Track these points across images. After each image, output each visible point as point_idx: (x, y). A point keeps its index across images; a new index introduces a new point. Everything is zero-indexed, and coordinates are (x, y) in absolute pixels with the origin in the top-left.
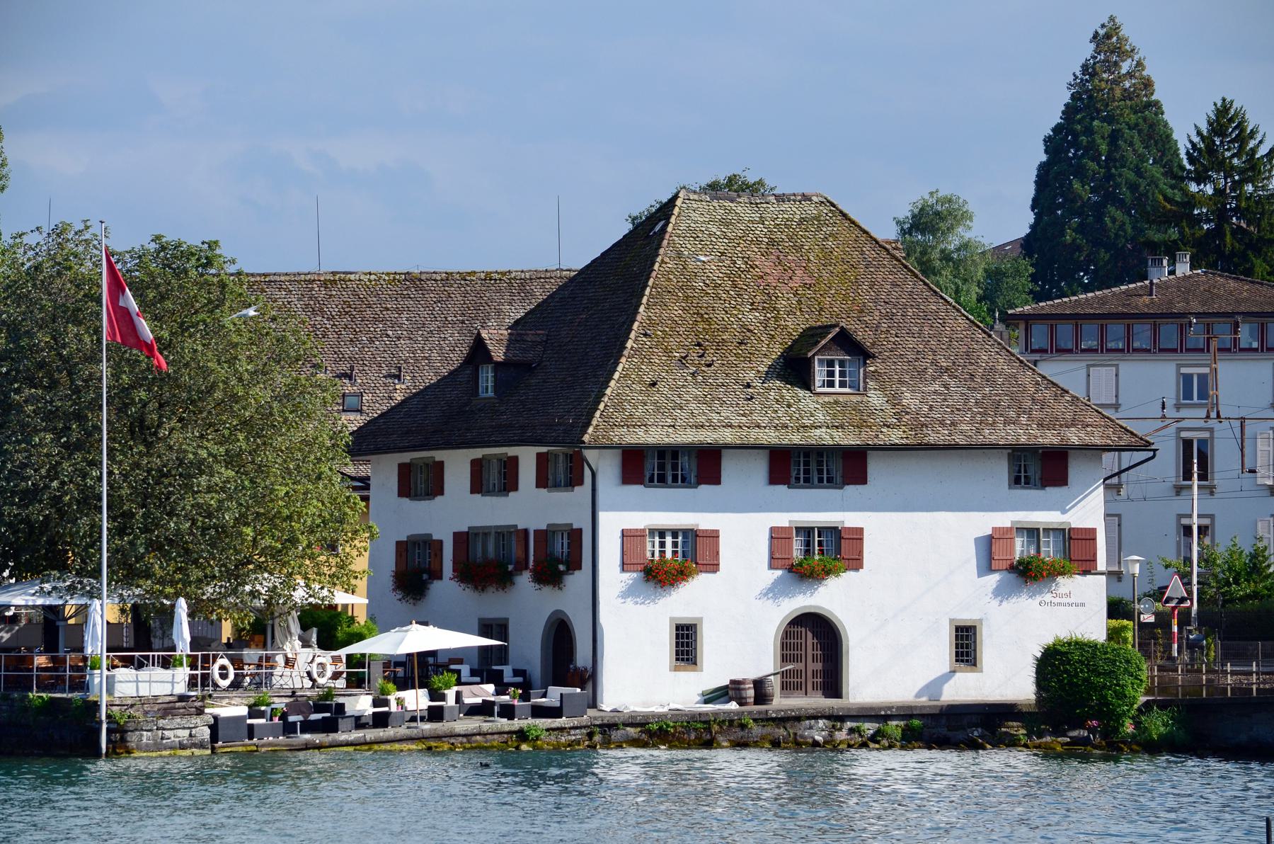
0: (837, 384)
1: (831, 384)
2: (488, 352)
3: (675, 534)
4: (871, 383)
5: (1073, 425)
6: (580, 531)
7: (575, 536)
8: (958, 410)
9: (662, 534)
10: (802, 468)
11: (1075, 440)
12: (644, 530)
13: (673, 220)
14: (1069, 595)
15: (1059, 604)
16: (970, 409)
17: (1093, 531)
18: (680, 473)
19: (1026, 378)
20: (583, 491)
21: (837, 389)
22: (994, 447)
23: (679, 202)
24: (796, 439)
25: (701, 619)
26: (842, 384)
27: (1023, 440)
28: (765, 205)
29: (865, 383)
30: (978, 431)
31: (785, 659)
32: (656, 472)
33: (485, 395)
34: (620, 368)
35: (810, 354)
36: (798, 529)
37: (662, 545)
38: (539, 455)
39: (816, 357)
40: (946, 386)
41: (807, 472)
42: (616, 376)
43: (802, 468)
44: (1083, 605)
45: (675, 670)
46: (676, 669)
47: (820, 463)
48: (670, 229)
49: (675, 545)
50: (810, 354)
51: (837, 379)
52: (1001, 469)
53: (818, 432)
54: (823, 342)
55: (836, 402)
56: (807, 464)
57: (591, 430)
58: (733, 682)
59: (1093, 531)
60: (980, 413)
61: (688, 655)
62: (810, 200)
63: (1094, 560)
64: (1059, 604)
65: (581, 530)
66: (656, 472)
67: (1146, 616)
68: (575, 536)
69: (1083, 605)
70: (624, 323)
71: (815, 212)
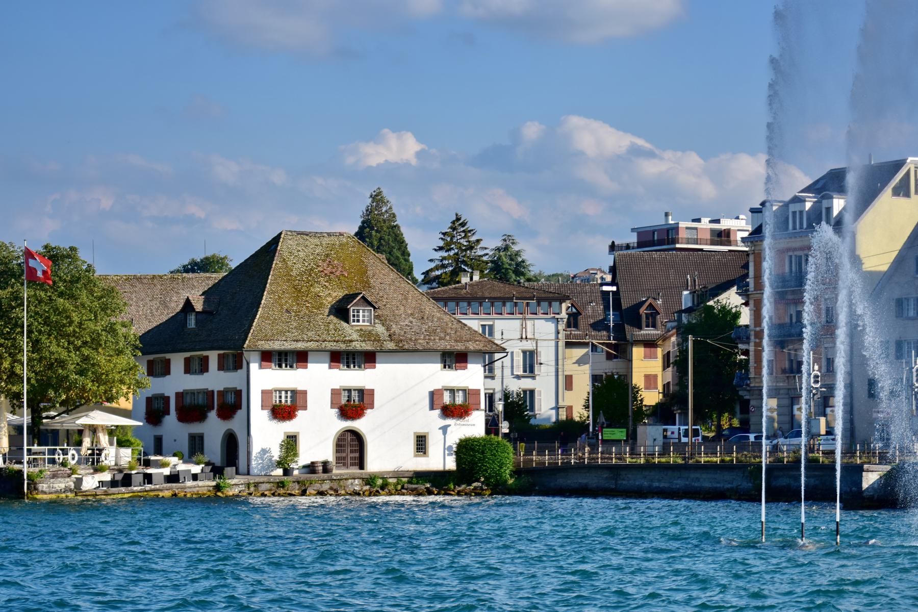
0: (361, 321)
1: (358, 321)
3: (286, 392)
5: (470, 341)
6: (240, 391)
7: (238, 393)
8: (418, 333)
9: (280, 391)
11: (471, 348)
13: (280, 244)
15: (464, 425)
17: (479, 390)
19: (446, 318)
20: (241, 373)
21: (361, 323)
22: (436, 351)
23: (282, 236)
24: (342, 347)
26: (364, 321)
27: (448, 347)
29: (374, 321)
31: (337, 451)
33: (190, 327)
34: (259, 313)
36: (344, 390)
37: (280, 397)
38: (219, 355)
40: (411, 322)
44: (474, 425)
47: (354, 359)
48: (279, 248)
49: (286, 397)
50: (349, 307)
51: (361, 319)
55: (361, 330)
57: (247, 342)
58: (312, 463)
59: (479, 390)
62: (343, 235)
63: (480, 404)
64: (464, 425)
65: (240, 391)
68: (238, 393)
69: (474, 425)
70: (259, 293)
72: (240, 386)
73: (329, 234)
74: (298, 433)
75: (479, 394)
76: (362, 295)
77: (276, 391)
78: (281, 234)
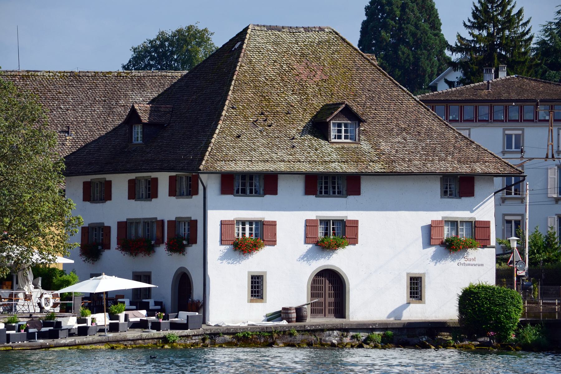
2: (139, 117)
3: (251, 223)
4: (362, 137)
6: (196, 221)
7: (193, 224)
10: (323, 186)
12: (233, 221)
13: (246, 41)
14: (474, 259)
15: (469, 265)
16: (419, 152)
17: (488, 223)
18: (254, 188)
21: (343, 140)
25: (266, 273)
28: (298, 34)
30: (424, 165)
32: (240, 188)
33: (136, 142)
34: (219, 127)
35: (328, 120)
39: (331, 122)
41: (326, 188)
42: (217, 131)
43: (323, 186)
44: (482, 265)
45: (251, 302)
46: (251, 301)
47: (334, 183)
48: (244, 46)
50: (328, 120)
51: (343, 134)
52: (436, 187)
53: (333, 165)
54: (336, 113)
56: (326, 183)
59: (488, 223)
60: (424, 154)
61: (258, 293)
62: (324, 31)
63: (489, 240)
64: (469, 265)
65: (196, 221)
66: (240, 188)
67: (520, 272)
68: (193, 224)
71: (327, 38)
72: (197, 216)
73: (307, 30)
74: (266, 273)
75: (489, 227)
76: (344, 106)
77: (238, 222)
78: (247, 28)
